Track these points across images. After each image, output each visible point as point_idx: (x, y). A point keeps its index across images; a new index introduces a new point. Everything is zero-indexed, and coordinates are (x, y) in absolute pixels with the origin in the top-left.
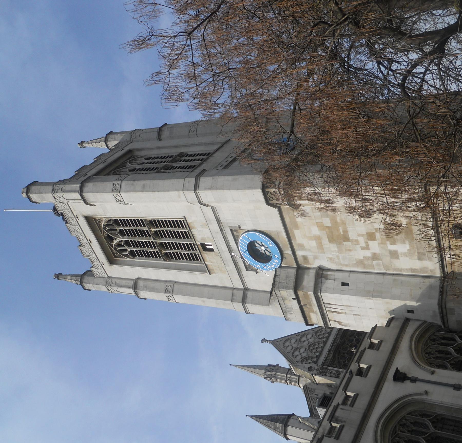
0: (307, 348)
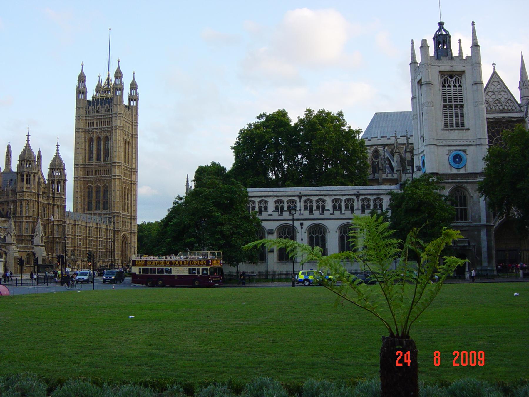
0: (496, 99)
